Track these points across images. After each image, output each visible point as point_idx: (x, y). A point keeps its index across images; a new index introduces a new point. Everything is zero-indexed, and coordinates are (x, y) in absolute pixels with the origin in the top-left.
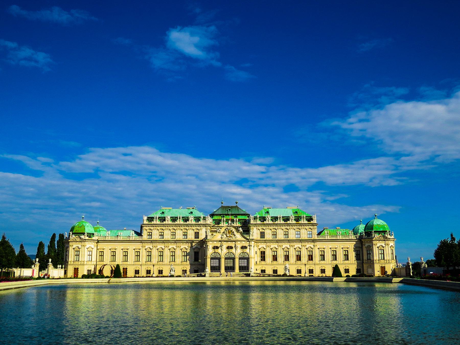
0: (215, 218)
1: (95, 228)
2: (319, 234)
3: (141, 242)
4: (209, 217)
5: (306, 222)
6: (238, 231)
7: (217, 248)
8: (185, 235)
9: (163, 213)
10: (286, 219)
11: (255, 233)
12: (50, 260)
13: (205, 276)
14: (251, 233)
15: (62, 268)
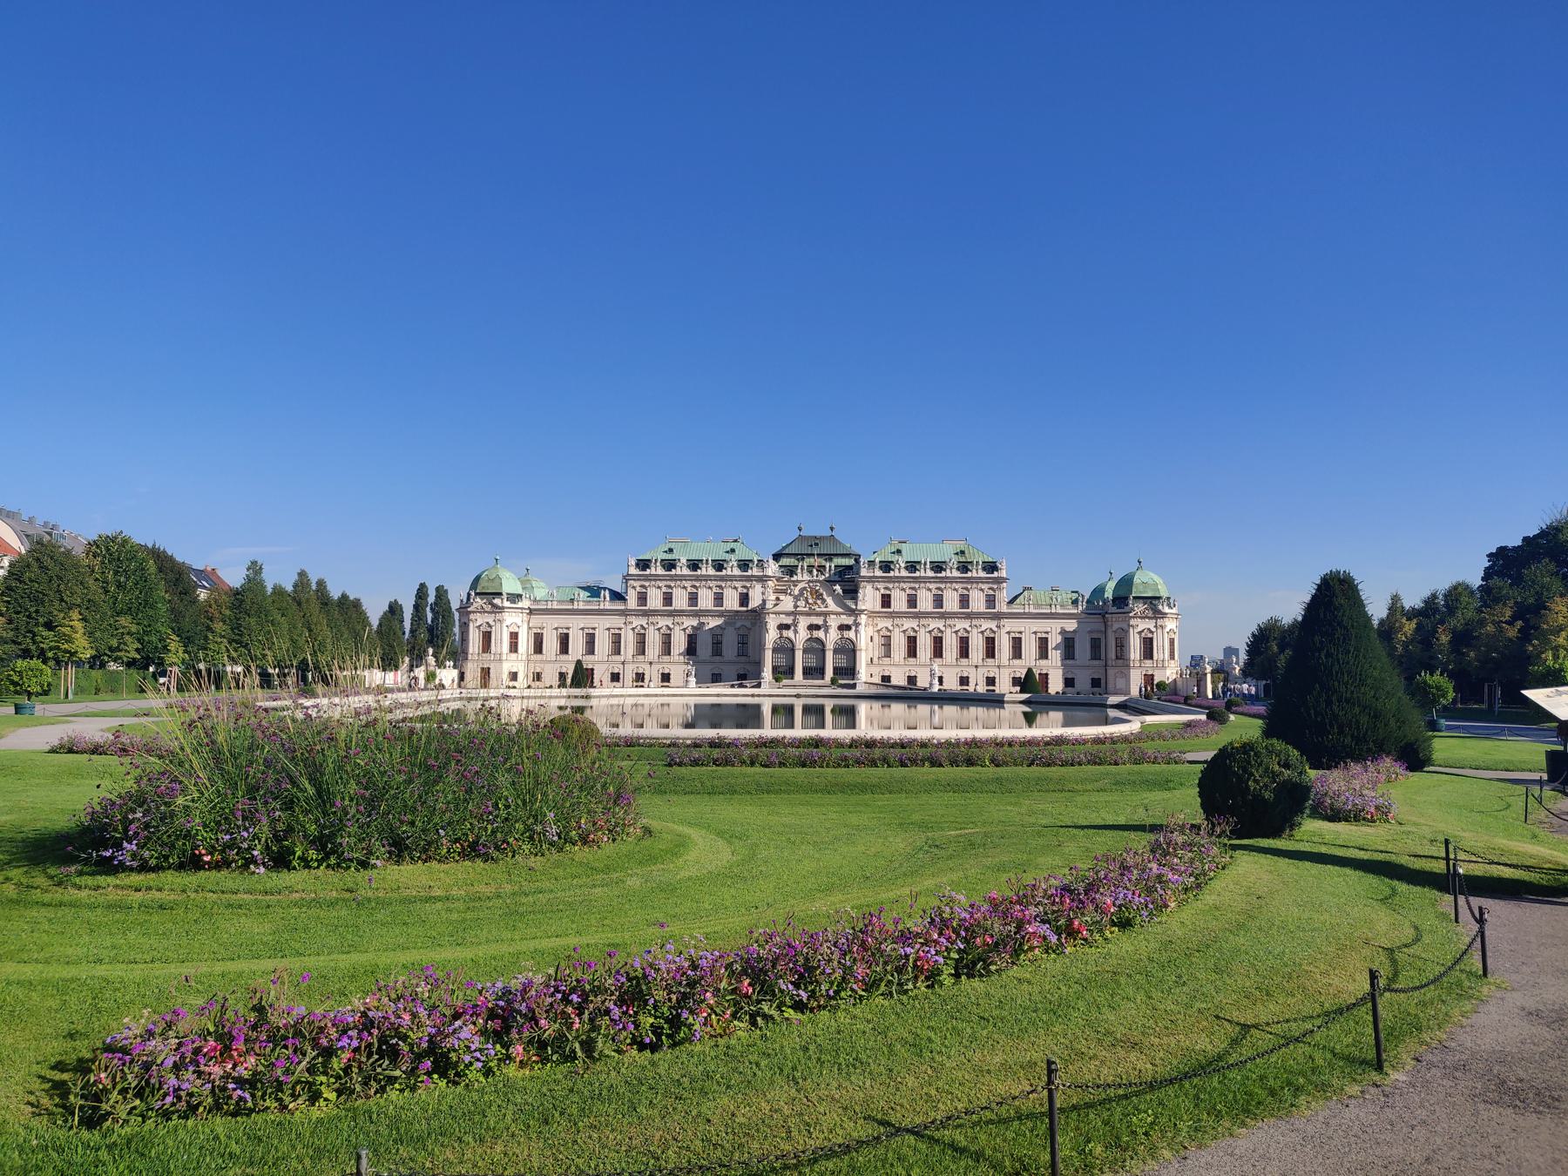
0: (785, 561)
1: (522, 583)
2: (1011, 602)
3: (624, 613)
4: (771, 561)
5: (982, 574)
6: (832, 593)
7: (787, 627)
8: (719, 599)
9: (671, 550)
10: (938, 567)
11: (869, 597)
12: (431, 651)
13: (759, 686)
14: (860, 596)
15: (455, 667)
